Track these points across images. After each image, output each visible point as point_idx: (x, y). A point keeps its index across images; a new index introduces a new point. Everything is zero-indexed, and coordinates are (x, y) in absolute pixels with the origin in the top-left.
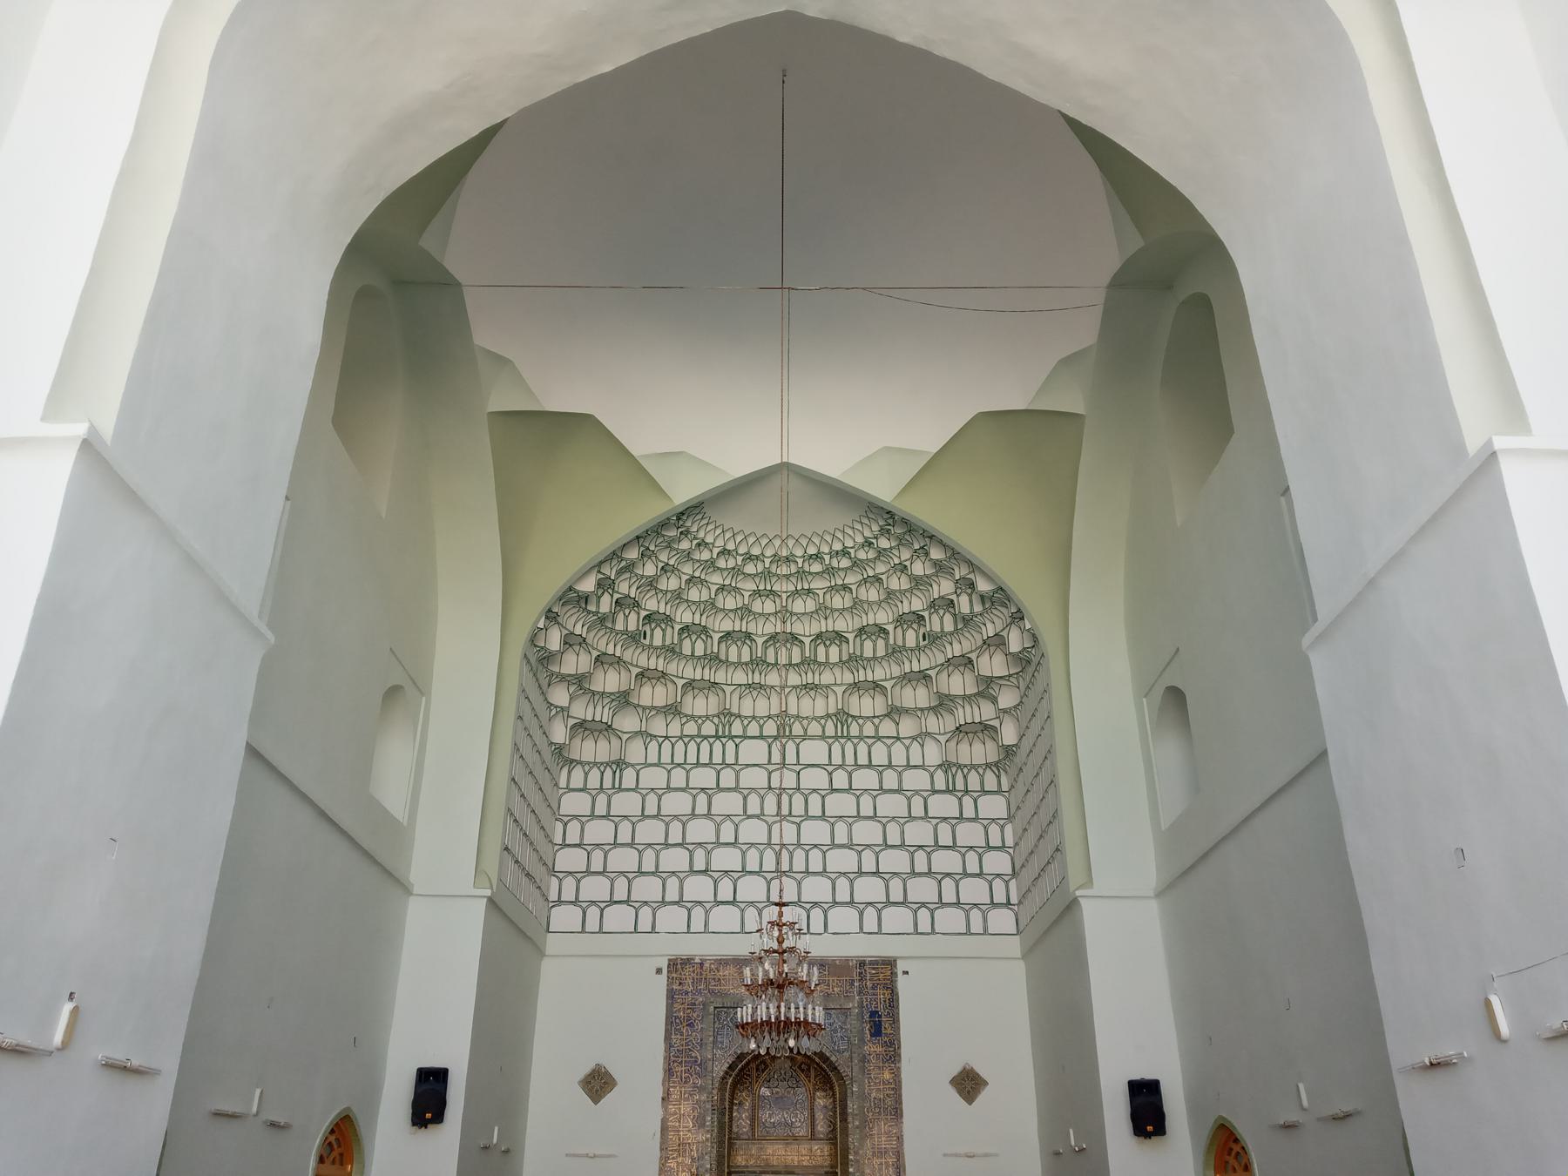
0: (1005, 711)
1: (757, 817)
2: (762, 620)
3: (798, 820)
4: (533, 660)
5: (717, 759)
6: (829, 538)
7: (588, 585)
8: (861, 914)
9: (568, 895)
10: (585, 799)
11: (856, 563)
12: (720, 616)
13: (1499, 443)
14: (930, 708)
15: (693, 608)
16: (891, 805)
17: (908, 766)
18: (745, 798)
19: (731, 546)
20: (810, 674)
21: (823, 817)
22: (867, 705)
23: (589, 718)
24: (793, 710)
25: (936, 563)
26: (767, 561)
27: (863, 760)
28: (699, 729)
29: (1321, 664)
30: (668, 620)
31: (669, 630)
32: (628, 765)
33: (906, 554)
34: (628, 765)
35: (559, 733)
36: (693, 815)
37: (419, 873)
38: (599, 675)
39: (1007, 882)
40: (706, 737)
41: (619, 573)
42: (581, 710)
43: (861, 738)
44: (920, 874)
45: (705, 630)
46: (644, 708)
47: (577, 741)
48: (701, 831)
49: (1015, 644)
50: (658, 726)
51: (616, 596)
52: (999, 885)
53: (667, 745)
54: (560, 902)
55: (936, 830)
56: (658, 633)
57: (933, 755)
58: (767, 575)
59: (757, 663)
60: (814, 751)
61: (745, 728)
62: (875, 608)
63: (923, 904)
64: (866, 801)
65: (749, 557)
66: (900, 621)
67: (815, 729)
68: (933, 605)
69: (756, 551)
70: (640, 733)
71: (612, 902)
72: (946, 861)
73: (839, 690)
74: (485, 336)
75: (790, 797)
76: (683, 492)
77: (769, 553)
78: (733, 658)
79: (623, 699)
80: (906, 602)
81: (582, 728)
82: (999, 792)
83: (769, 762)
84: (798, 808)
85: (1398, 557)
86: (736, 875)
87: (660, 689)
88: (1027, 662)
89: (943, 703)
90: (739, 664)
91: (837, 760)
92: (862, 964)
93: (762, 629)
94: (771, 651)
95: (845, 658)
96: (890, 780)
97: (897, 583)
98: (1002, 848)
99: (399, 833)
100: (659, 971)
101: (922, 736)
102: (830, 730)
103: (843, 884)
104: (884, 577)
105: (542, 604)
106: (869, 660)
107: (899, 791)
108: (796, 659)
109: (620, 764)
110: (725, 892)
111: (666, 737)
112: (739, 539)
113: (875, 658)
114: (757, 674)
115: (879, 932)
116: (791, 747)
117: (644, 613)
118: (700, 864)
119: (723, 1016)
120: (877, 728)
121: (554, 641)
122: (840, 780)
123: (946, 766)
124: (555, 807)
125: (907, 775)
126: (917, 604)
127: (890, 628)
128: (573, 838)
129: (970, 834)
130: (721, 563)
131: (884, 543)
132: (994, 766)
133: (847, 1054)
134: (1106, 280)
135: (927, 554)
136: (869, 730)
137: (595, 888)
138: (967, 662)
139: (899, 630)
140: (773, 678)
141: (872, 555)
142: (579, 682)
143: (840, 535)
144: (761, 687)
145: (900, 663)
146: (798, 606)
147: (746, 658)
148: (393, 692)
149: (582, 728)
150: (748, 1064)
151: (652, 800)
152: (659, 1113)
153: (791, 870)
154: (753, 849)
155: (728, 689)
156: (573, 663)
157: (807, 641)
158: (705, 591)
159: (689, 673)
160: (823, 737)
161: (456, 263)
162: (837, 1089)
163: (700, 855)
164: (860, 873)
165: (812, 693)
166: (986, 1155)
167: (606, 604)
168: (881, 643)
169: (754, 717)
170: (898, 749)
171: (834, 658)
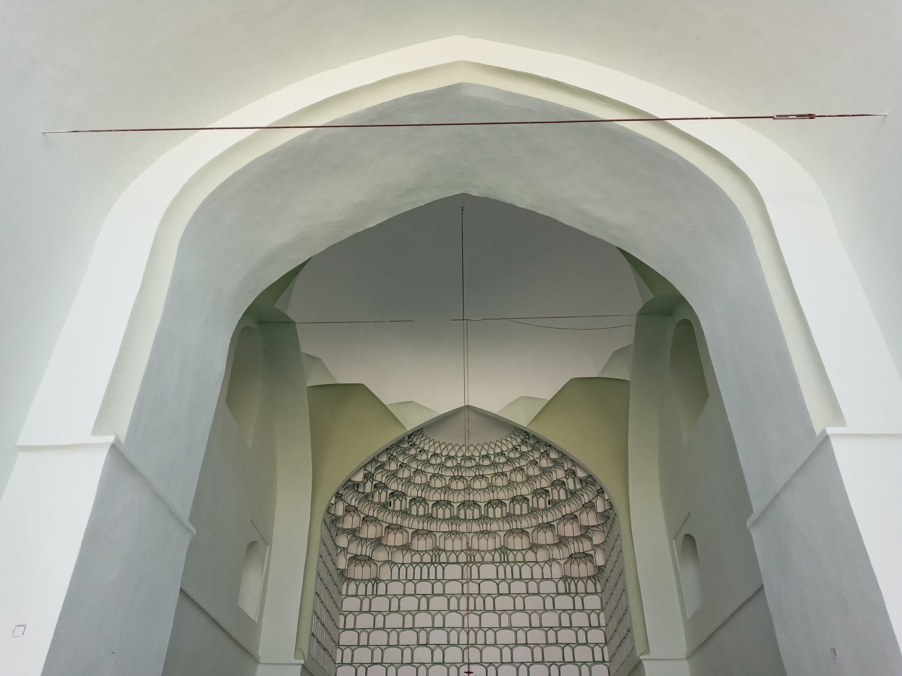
0: (597, 546)
1: (456, 611)
2: (457, 493)
3: (479, 613)
4: (328, 521)
5: (432, 576)
6: (493, 446)
7: (359, 478)
8: (518, 669)
9: (347, 660)
10: (357, 601)
11: (509, 460)
12: (433, 491)
13: (830, 431)
16: (534, 603)
17: (543, 579)
18: (449, 600)
19: (438, 451)
20: (485, 525)
21: (494, 611)
22: (518, 543)
23: (359, 553)
24: (475, 547)
25: (554, 461)
26: (459, 459)
27: (517, 576)
28: (422, 559)
29: (756, 535)
30: (404, 495)
33: (536, 455)
35: (342, 563)
36: (419, 610)
37: (263, 651)
38: (365, 528)
39: (602, 648)
40: (425, 564)
41: (376, 469)
42: (354, 549)
43: (515, 562)
44: (552, 644)
45: (424, 500)
46: (390, 547)
47: (352, 567)
48: (423, 620)
49: (600, 509)
50: (398, 557)
51: (374, 482)
52: (597, 650)
53: (403, 568)
54: (342, 664)
55: (560, 617)
56: (398, 502)
57: (557, 571)
58: (459, 467)
59: (454, 519)
60: (488, 571)
61: (448, 558)
62: (521, 485)
63: (554, 663)
64: (519, 600)
65: (449, 457)
66: (535, 493)
67: (488, 558)
68: (553, 484)
69: (452, 454)
71: (373, 664)
72: (566, 636)
73: (502, 534)
74: (307, 347)
75: (475, 599)
76: (411, 424)
77: (460, 454)
78: (440, 516)
79: (378, 542)
80: (538, 482)
81: (355, 559)
82: (596, 593)
84: (480, 606)
85: (788, 484)
86: (444, 647)
87: (399, 535)
88: (608, 518)
89: (562, 541)
91: (501, 576)
93: (457, 499)
94: (462, 511)
95: (504, 515)
96: (533, 587)
97: (532, 471)
98: (599, 627)
99: (252, 627)
101: (550, 561)
103: (506, 651)
104: (525, 468)
105: (333, 491)
106: (518, 516)
107: (538, 594)
108: (477, 516)
109: (376, 580)
110: (438, 657)
111: (403, 564)
112: (443, 447)
113: (521, 515)
114: (454, 525)
116: (474, 568)
117: (390, 492)
118: (423, 640)
120: (524, 556)
121: (340, 510)
122: (504, 588)
123: (564, 578)
124: (339, 606)
126: (545, 484)
127: (530, 497)
128: (350, 625)
129: (580, 619)
130: (433, 461)
131: (524, 449)
132: (593, 578)
134: (636, 311)
135: (548, 455)
136: (519, 557)
137: (362, 655)
138: (573, 517)
139: (535, 498)
141: (517, 455)
142: (354, 533)
143: (499, 444)
144: (457, 532)
145: (536, 518)
146: (477, 485)
147: (448, 516)
148: (253, 544)
149: (355, 559)
151: (395, 601)
153: (476, 643)
154: (454, 631)
155: (438, 535)
156: (350, 522)
157: (482, 505)
158: (424, 478)
160: (493, 562)
161: (292, 313)
163: (423, 634)
164: (517, 644)
165: (486, 536)
167: (368, 488)
168: (525, 506)
169: (453, 551)
170: (537, 569)
171: (498, 515)
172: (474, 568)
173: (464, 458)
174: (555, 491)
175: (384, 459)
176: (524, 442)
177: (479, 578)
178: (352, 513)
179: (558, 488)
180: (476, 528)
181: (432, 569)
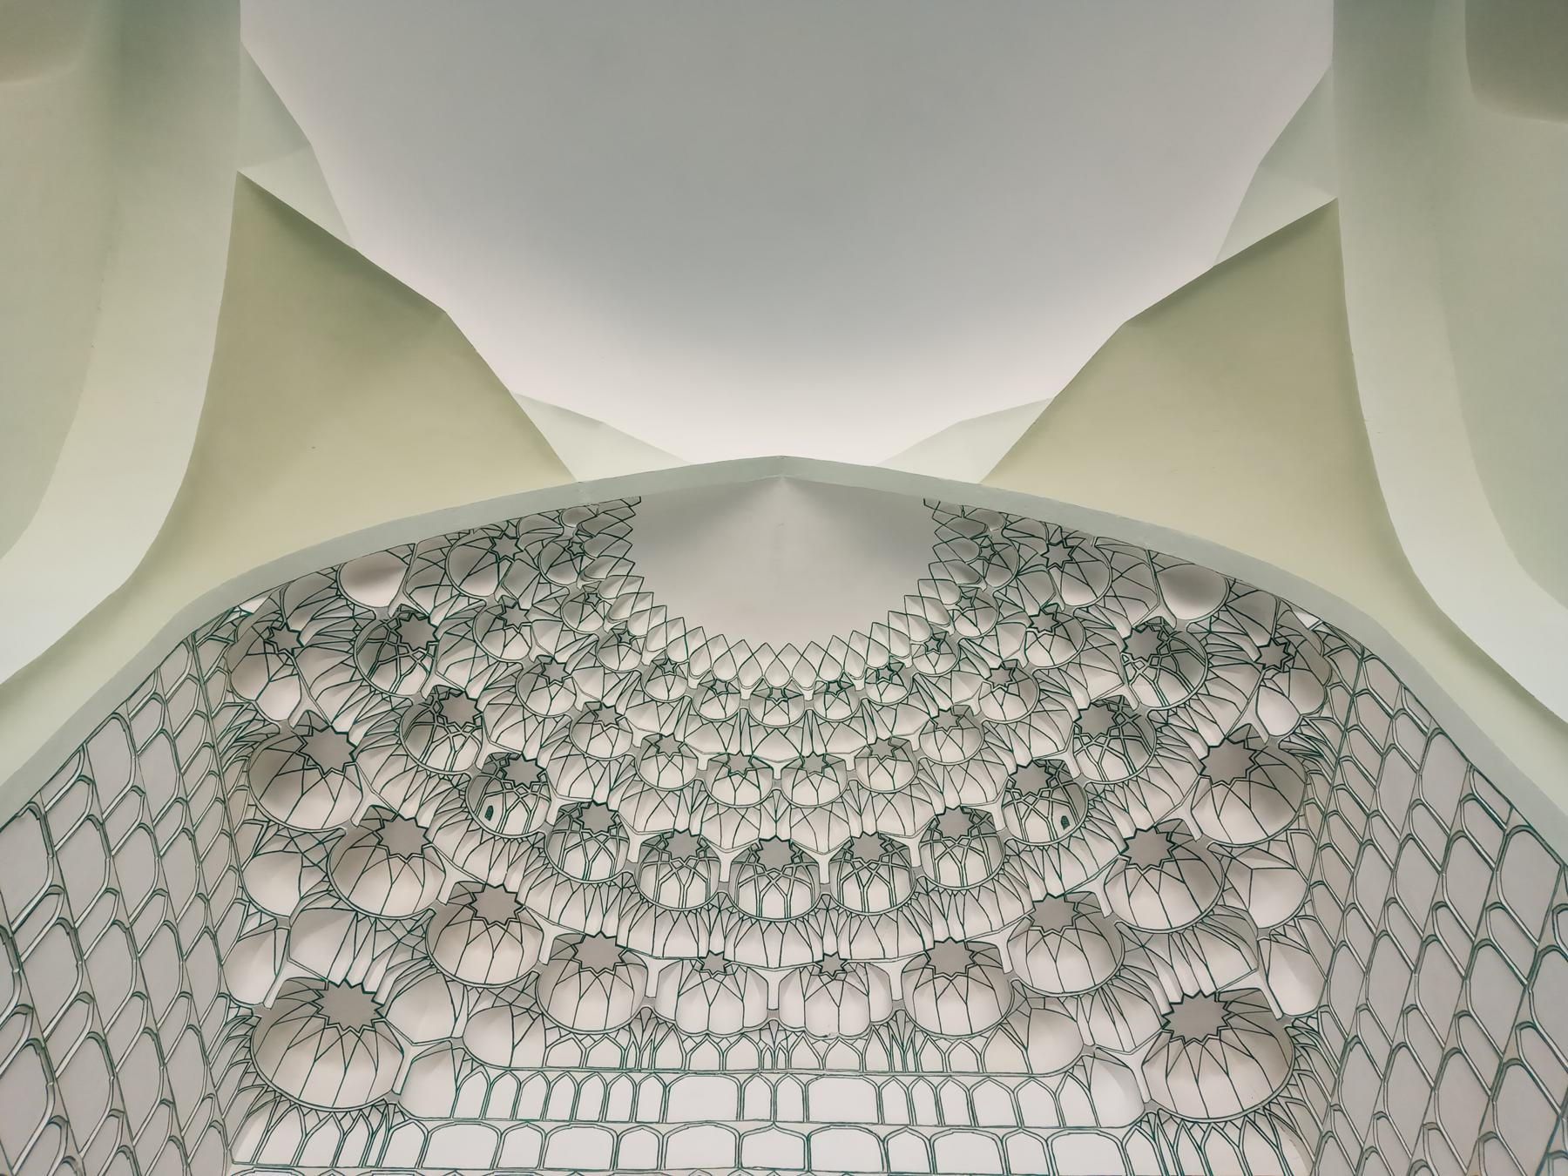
0: (1273, 935)
11: (917, 686)
12: (651, 802)
14: (1099, 990)
15: (597, 772)
17: (1063, 1127)
19: (678, 655)
20: (830, 940)
22: (955, 1012)
23: (337, 977)
24: (792, 1014)
26: (746, 694)
28: (585, 1056)
31: (543, 805)
32: (409, 1118)
34: (409, 1118)
40: (596, 1071)
42: (319, 954)
43: (948, 1074)
47: (301, 1059)
50: (492, 1043)
53: (507, 1086)
57: (1116, 1101)
58: (743, 722)
59: (720, 904)
60: (842, 1098)
61: (686, 1056)
62: (958, 776)
68: (1077, 731)
69: (725, 674)
70: (452, 1048)
73: (894, 970)
76: (592, 466)
77: (749, 680)
78: (670, 895)
83: (740, 1115)
90: (684, 911)
91: (896, 1111)
93: (729, 839)
95: (902, 893)
97: (1003, 709)
102: (876, 1057)
104: (973, 704)
111: (509, 1070)
113: (964, 889)
116: (789, 1092)
117: (489, 749)
120: (980, 1057)
123: (1153, 1119)
125: (1062, 1145)
131: (966, 629)
136: (962, 1059)
139: (1010, 811)
140: (749, 951)
141: (944, 665)
143: (880, 637)
144: (727, 968)
146: (804, 794)
159: (574, 919)
160: (863, 1072)
169: (708, 1034)
171: (878, 898)
172: (789, 1092)
173: (769, 695)
174: (1082, 757)
175: (485, 589)
176: (971, 601)
177: (806, 1118)
178: (335, 779)
179: (1095, 751)
180: (797, 953)
181: (622, 1089)
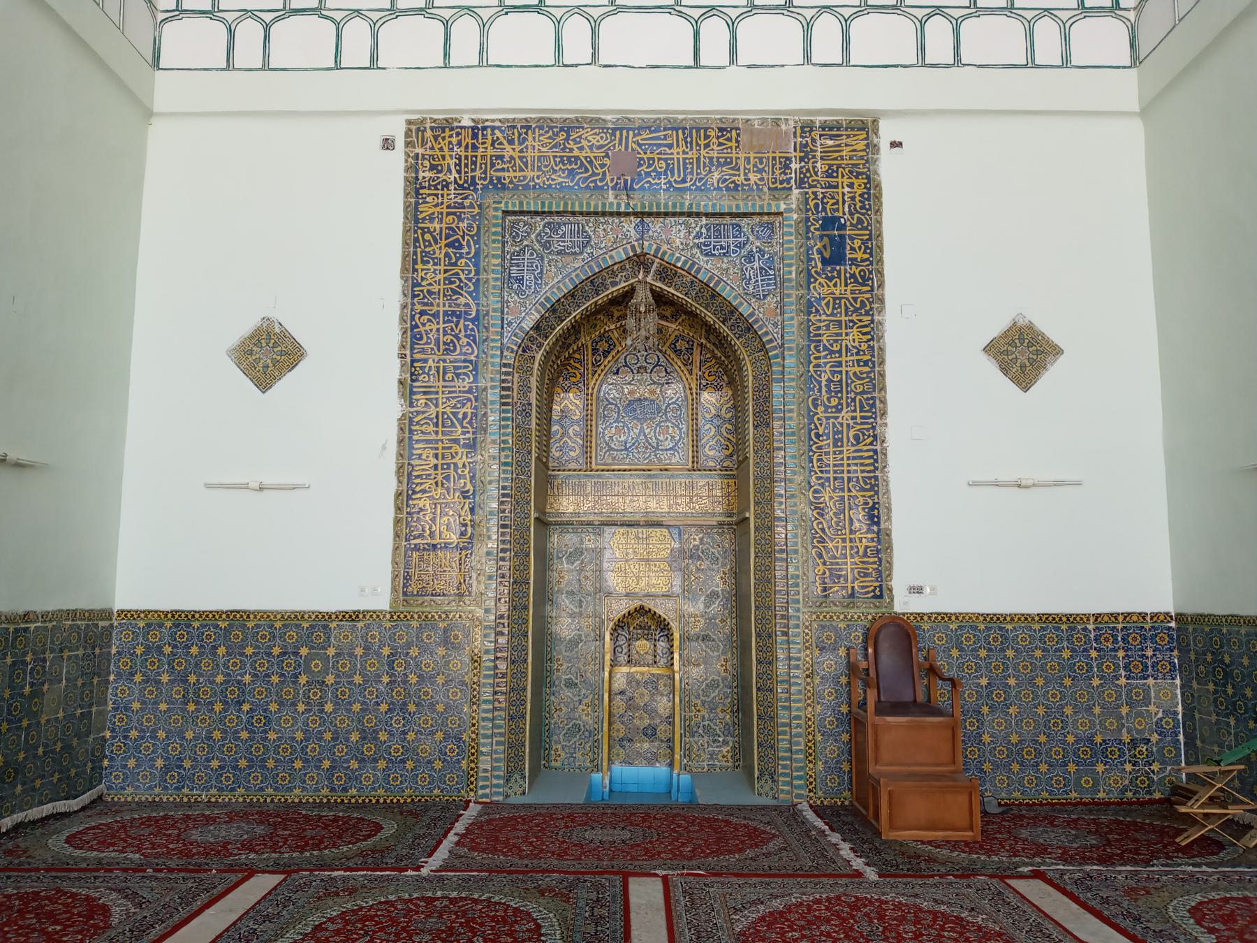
8: (808, 28)
54: (179, 12)
92: (806, 128)
100: (388, 144)
115: (846, 62)
119: (523, 229)
133: (772, 301)
150: (575, 329)
152: (394, 407)
162: (749, 371)
166: (1058, 484)
